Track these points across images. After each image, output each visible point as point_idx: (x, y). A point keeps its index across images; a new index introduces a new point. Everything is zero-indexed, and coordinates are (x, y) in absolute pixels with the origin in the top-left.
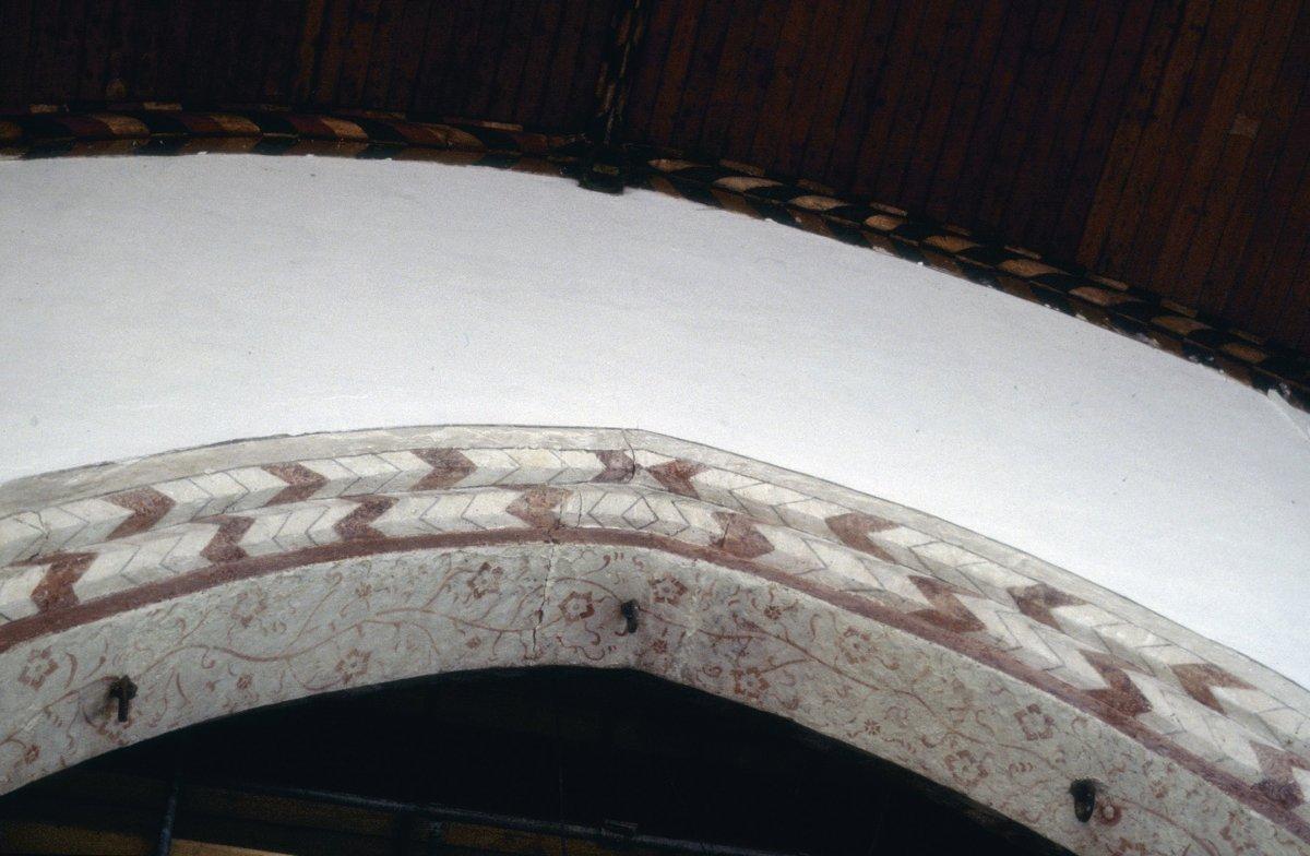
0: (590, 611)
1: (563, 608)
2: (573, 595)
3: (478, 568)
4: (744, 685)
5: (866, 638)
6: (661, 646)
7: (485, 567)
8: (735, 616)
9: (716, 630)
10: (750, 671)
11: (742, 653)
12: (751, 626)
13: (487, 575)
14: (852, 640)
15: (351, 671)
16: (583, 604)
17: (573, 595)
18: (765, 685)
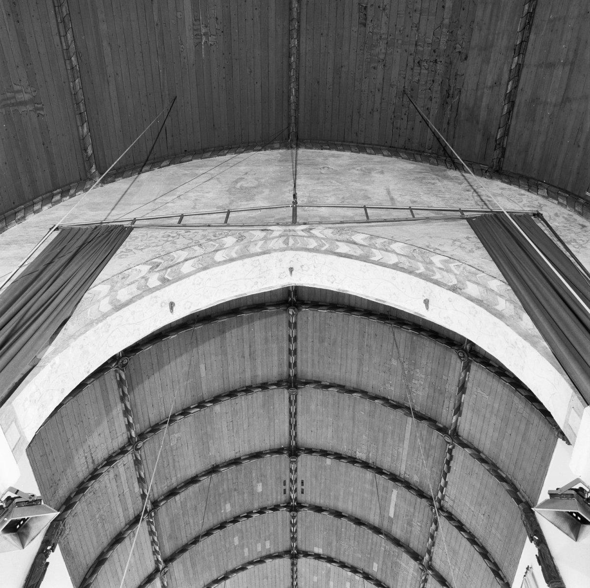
0: (302, 266)
1: (309, 268)
2: (307, 271)
3: (334, 282)
4: (258, 263)
5: (233, 292)
6: (280, 261)
7: (332, 283)
8: (265, 277)
9: (268, 272)
10: (257, 266)
11: (260, 270)
12: (260, 277)
13: (331, 280)
14: (235, 289)
15: (365, 268)
16: (304, 269)
17: (307, 271)
18: (252, 265)
